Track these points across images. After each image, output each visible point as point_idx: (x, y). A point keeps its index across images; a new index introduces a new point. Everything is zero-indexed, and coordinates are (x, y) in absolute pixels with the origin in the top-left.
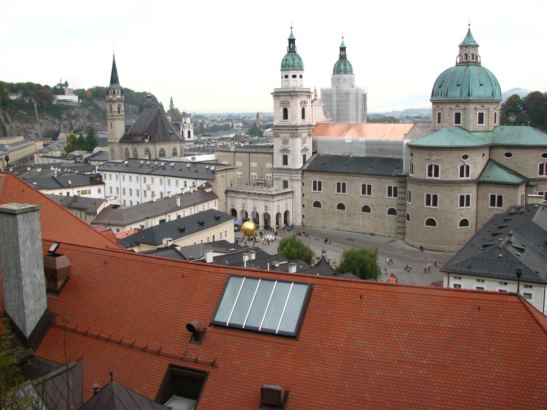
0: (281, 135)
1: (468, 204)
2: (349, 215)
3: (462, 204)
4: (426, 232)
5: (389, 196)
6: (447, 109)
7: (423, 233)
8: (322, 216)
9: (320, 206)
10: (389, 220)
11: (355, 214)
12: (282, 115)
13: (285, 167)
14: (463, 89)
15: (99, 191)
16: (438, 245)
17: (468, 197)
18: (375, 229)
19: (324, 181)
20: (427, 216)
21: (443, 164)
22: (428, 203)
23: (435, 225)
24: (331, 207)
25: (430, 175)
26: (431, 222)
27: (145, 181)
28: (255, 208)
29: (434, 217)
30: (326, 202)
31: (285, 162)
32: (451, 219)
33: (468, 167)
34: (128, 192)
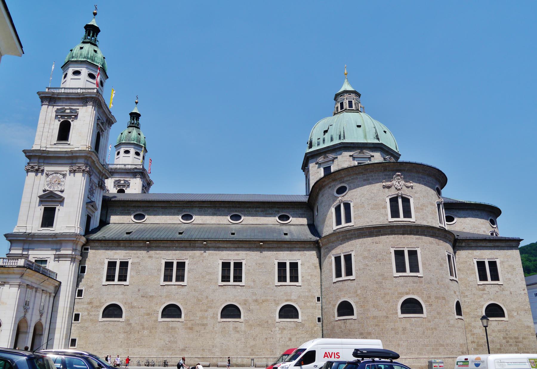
2: (191, 329)
4: (404, 329)
6: (346, 156)
7: (397, 333)
8: (122, 336)
9: (120, 315)
11: (205, 325)
13: (47, 231)
14: (367, 130)
16: (432, 354)
18: (251, 354)
19: (136, 260)
20: (401, 294)
21: (416, 195)
23: (421, 312)
24: (148, 314)
25: (395, 213)
29: (418, 293)
30: (135, 304)
32: (444, 298)
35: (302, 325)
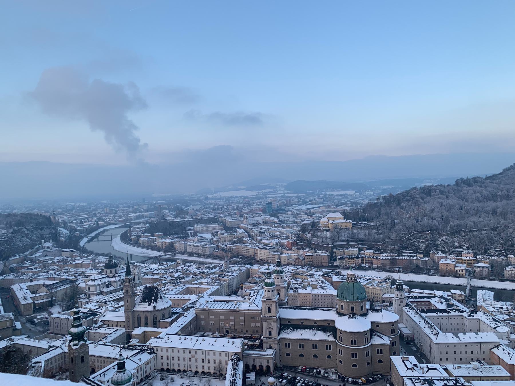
0: (268, 321)
1: (369, 355)
3: (367, 356)
5: (327, 349)
10: (327, 361)
12: (267, 310)
13: (270, 337)
15: (154, 360)
17: (369, 351)
22: (353, 357)
26: (354, 366)
27: (190, 353)
28: (261, 363)
31: (270, 333)
33: (367, 338)
34: (176, 359)
35: (332, 360)
